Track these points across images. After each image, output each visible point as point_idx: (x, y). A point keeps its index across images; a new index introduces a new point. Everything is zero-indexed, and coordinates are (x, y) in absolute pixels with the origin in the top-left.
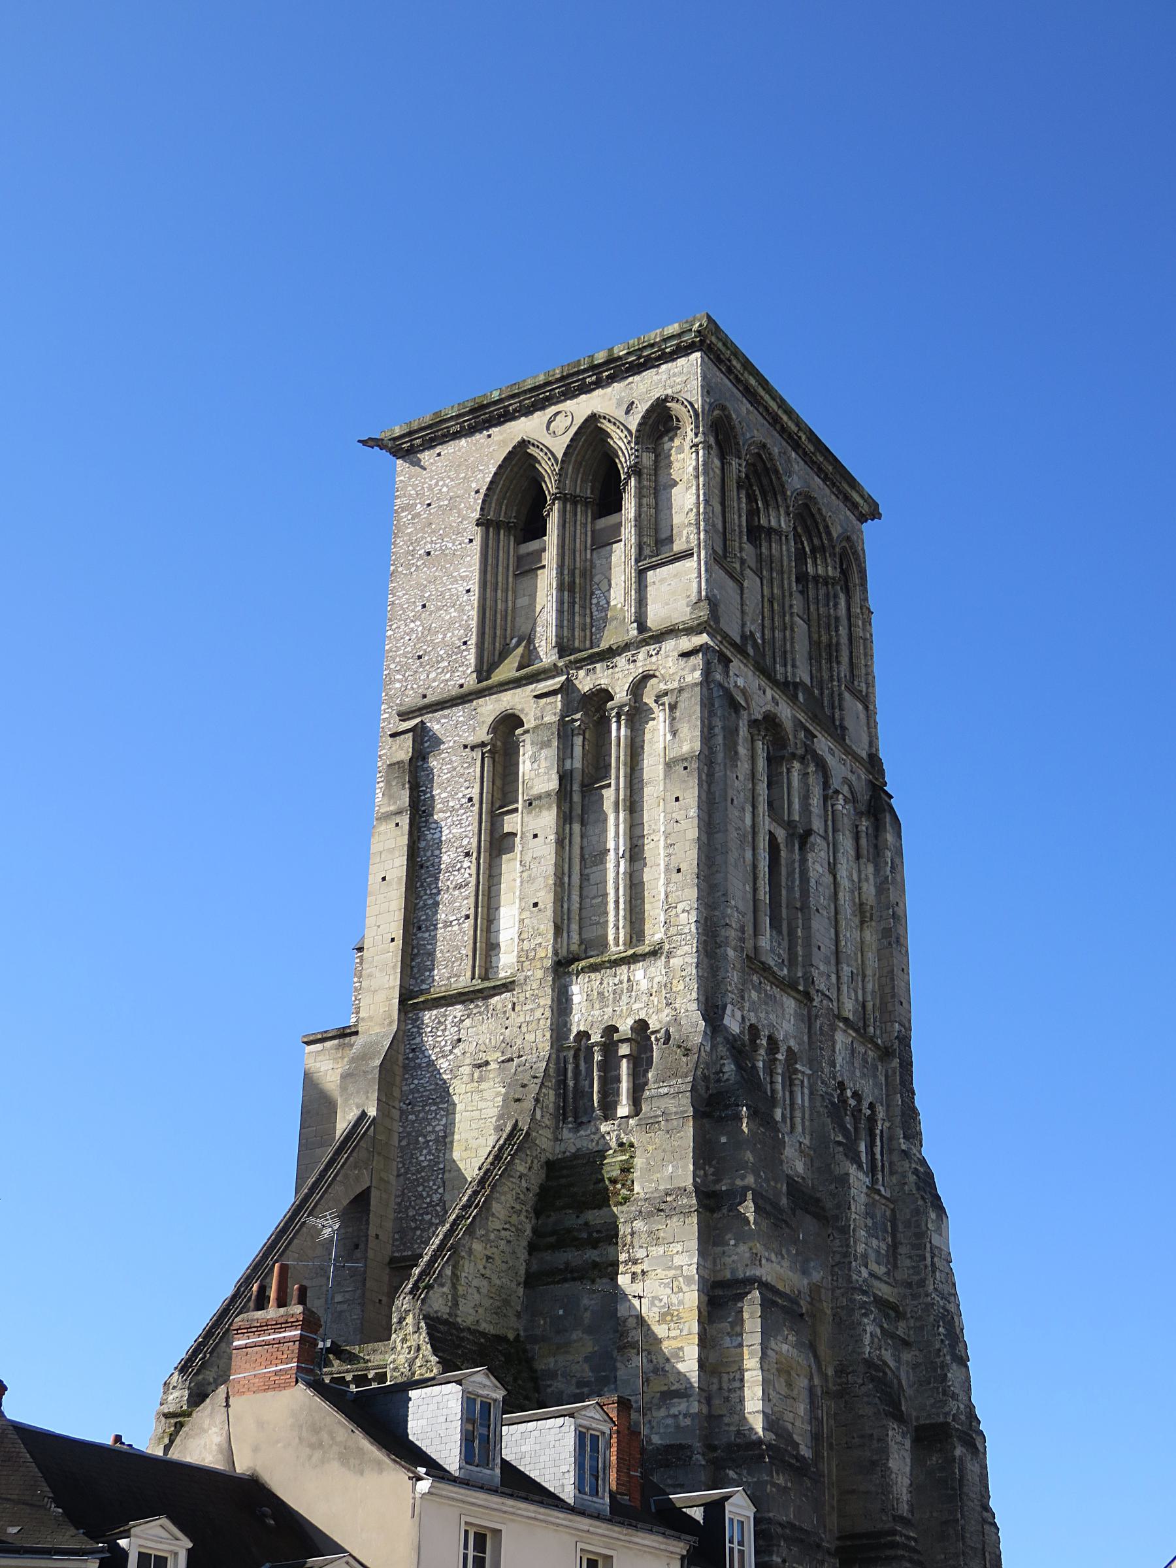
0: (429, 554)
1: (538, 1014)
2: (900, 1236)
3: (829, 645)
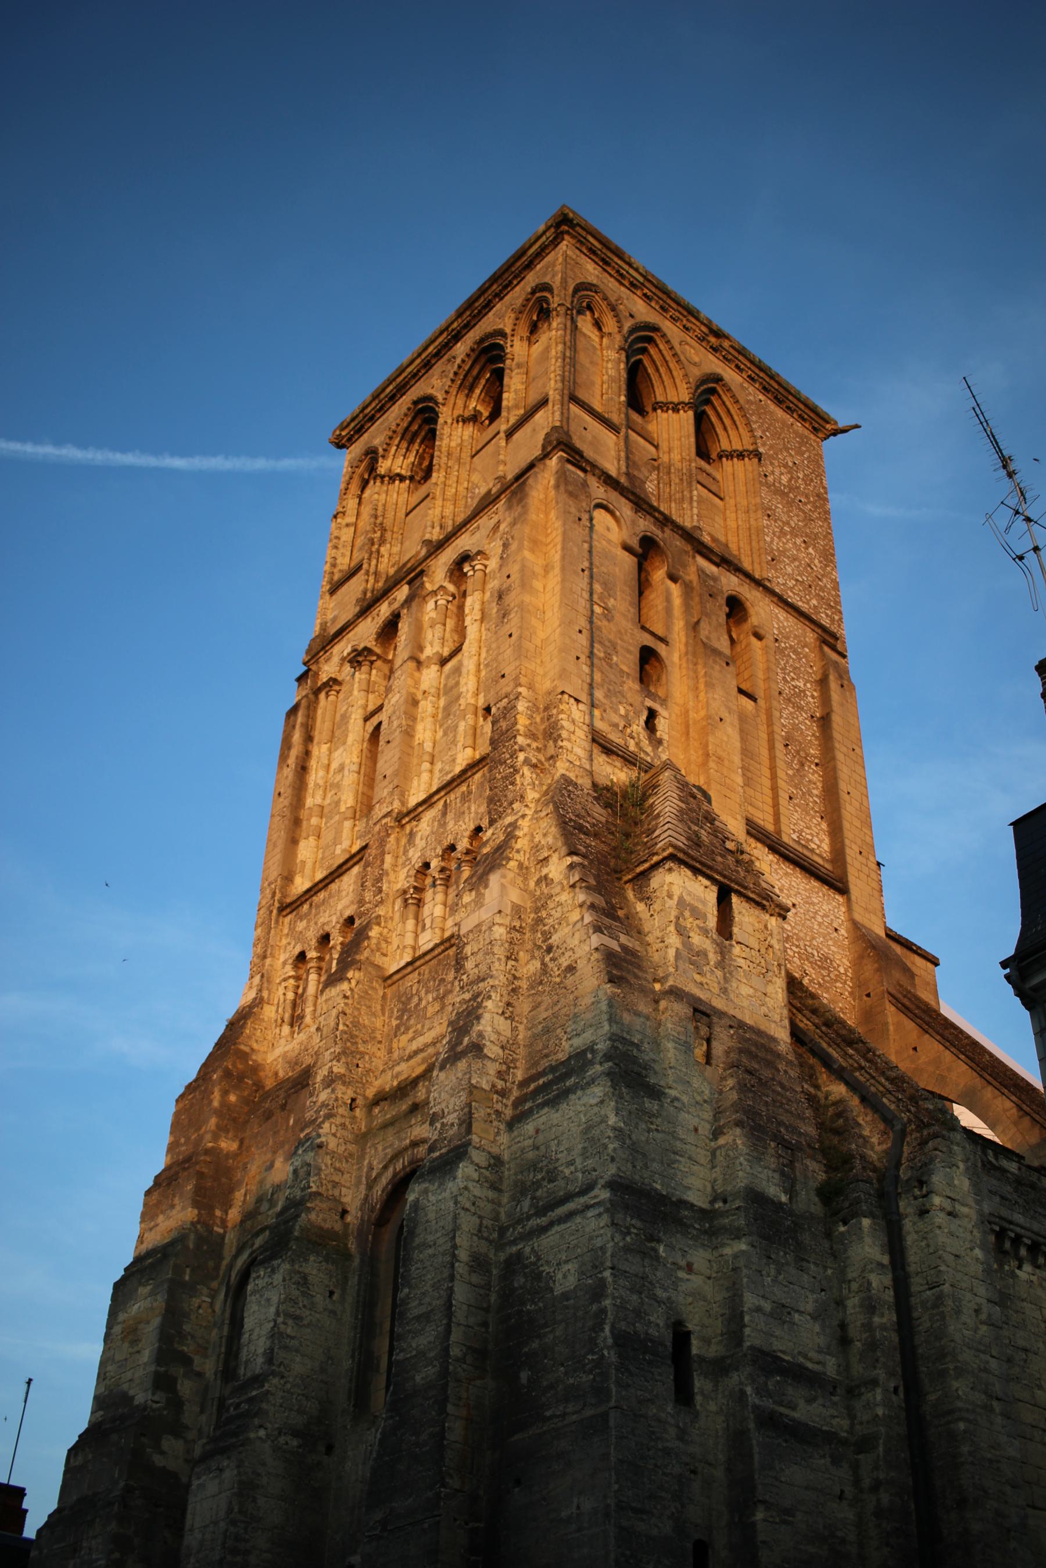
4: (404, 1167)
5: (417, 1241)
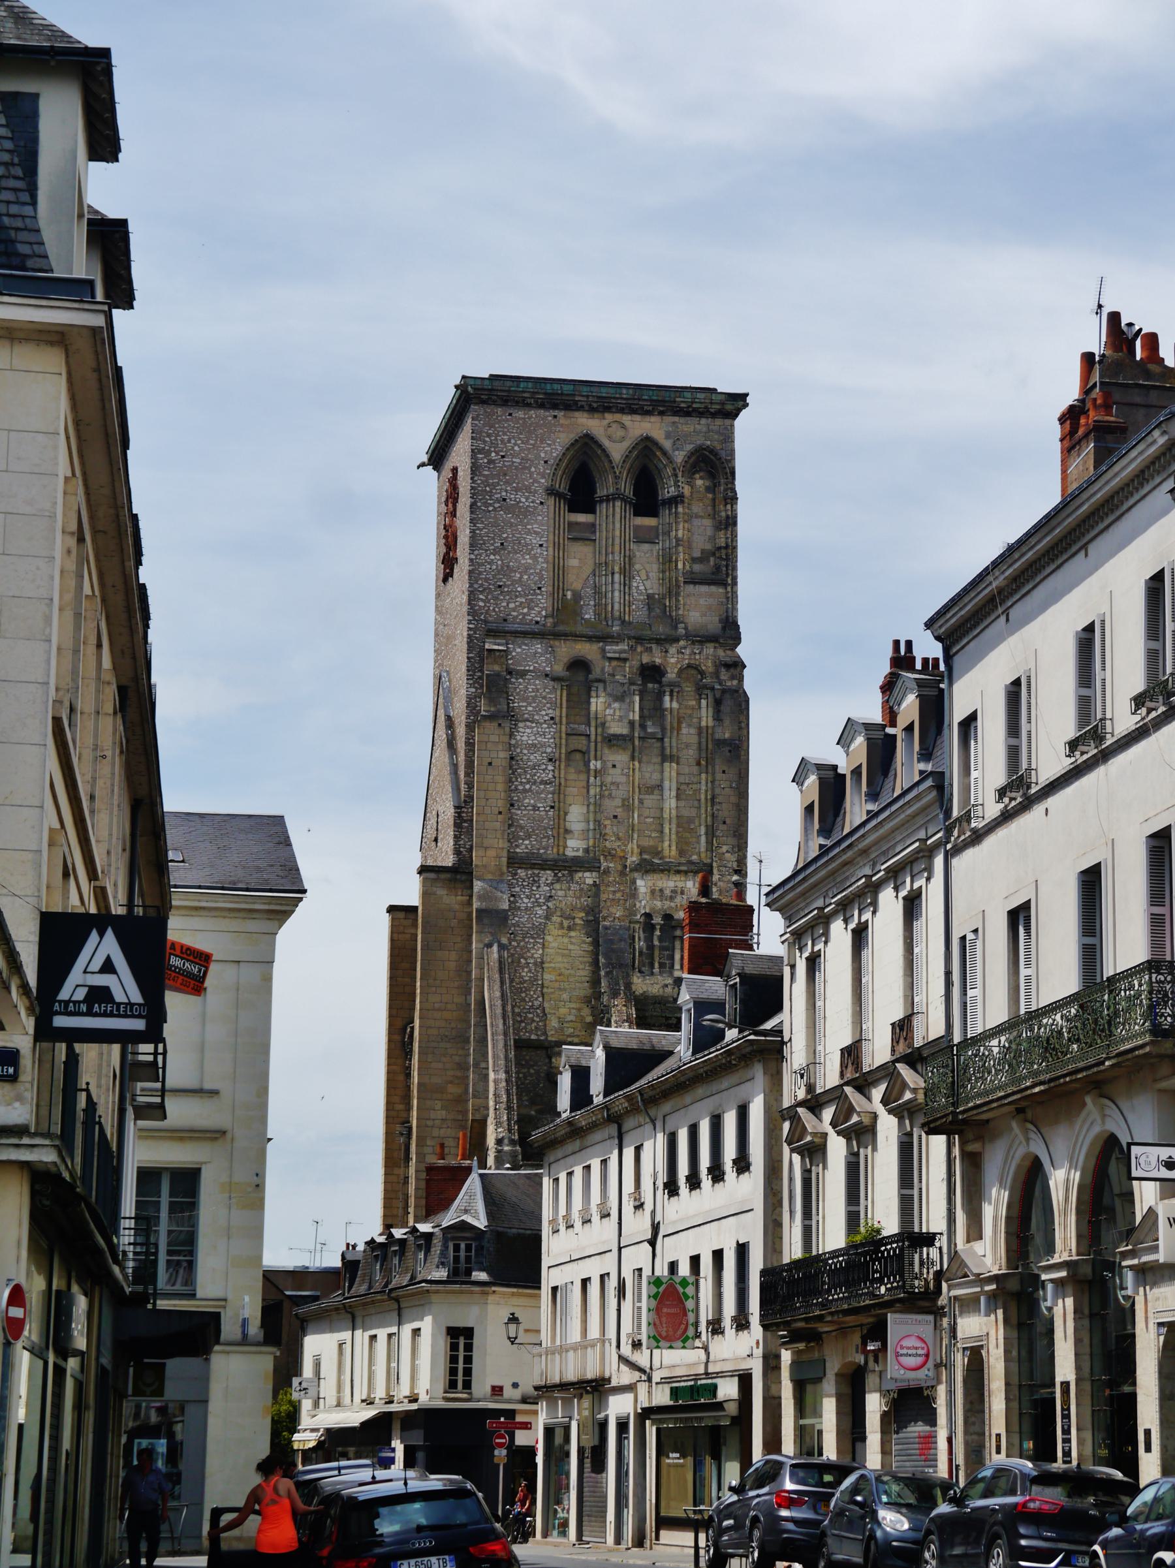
0: (504, 500)
1: (618, 895)
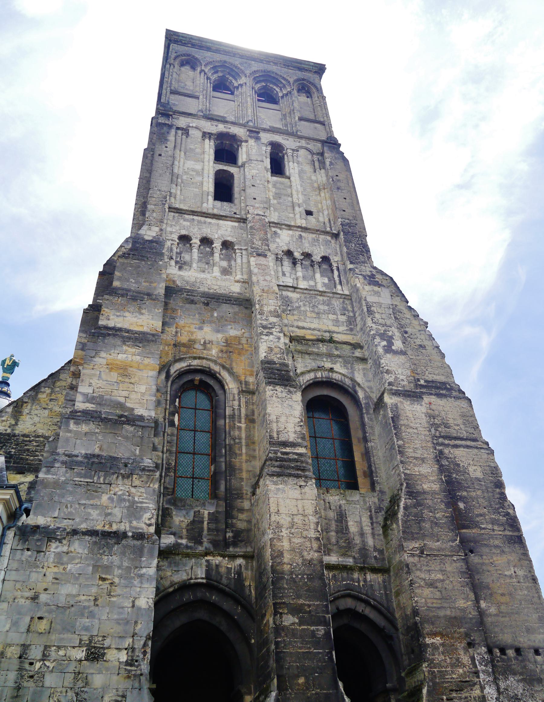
2: (356, 309)
3: (290, 113)
4: (322, 377)
5: (402, 422)
